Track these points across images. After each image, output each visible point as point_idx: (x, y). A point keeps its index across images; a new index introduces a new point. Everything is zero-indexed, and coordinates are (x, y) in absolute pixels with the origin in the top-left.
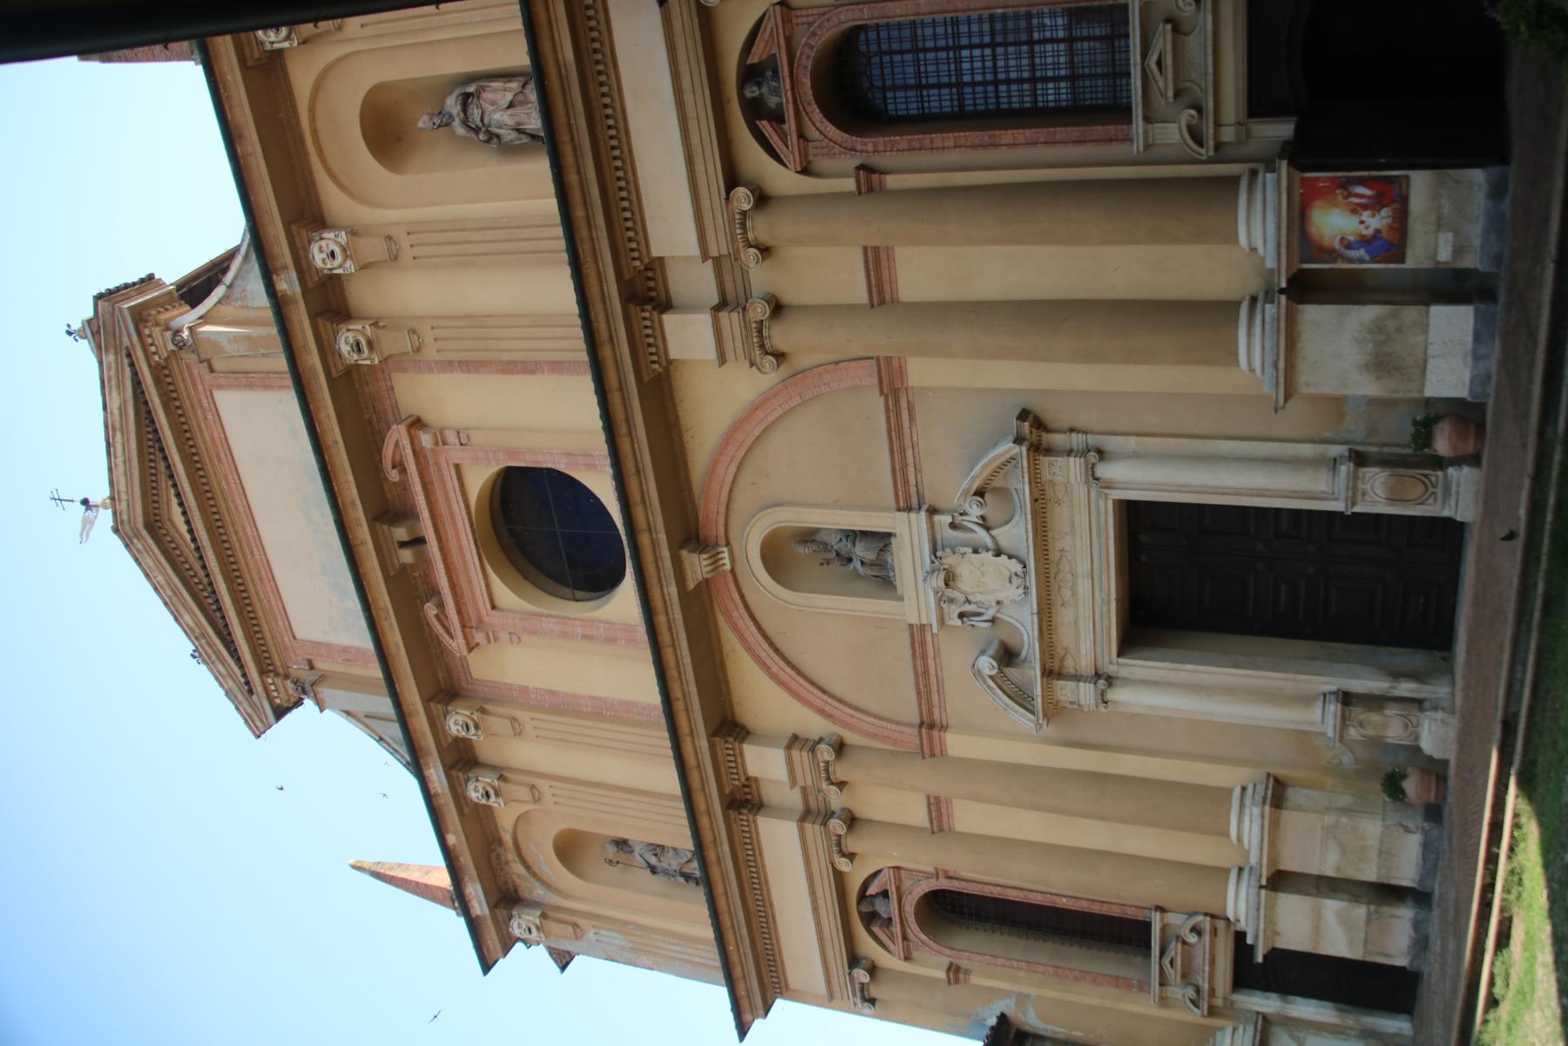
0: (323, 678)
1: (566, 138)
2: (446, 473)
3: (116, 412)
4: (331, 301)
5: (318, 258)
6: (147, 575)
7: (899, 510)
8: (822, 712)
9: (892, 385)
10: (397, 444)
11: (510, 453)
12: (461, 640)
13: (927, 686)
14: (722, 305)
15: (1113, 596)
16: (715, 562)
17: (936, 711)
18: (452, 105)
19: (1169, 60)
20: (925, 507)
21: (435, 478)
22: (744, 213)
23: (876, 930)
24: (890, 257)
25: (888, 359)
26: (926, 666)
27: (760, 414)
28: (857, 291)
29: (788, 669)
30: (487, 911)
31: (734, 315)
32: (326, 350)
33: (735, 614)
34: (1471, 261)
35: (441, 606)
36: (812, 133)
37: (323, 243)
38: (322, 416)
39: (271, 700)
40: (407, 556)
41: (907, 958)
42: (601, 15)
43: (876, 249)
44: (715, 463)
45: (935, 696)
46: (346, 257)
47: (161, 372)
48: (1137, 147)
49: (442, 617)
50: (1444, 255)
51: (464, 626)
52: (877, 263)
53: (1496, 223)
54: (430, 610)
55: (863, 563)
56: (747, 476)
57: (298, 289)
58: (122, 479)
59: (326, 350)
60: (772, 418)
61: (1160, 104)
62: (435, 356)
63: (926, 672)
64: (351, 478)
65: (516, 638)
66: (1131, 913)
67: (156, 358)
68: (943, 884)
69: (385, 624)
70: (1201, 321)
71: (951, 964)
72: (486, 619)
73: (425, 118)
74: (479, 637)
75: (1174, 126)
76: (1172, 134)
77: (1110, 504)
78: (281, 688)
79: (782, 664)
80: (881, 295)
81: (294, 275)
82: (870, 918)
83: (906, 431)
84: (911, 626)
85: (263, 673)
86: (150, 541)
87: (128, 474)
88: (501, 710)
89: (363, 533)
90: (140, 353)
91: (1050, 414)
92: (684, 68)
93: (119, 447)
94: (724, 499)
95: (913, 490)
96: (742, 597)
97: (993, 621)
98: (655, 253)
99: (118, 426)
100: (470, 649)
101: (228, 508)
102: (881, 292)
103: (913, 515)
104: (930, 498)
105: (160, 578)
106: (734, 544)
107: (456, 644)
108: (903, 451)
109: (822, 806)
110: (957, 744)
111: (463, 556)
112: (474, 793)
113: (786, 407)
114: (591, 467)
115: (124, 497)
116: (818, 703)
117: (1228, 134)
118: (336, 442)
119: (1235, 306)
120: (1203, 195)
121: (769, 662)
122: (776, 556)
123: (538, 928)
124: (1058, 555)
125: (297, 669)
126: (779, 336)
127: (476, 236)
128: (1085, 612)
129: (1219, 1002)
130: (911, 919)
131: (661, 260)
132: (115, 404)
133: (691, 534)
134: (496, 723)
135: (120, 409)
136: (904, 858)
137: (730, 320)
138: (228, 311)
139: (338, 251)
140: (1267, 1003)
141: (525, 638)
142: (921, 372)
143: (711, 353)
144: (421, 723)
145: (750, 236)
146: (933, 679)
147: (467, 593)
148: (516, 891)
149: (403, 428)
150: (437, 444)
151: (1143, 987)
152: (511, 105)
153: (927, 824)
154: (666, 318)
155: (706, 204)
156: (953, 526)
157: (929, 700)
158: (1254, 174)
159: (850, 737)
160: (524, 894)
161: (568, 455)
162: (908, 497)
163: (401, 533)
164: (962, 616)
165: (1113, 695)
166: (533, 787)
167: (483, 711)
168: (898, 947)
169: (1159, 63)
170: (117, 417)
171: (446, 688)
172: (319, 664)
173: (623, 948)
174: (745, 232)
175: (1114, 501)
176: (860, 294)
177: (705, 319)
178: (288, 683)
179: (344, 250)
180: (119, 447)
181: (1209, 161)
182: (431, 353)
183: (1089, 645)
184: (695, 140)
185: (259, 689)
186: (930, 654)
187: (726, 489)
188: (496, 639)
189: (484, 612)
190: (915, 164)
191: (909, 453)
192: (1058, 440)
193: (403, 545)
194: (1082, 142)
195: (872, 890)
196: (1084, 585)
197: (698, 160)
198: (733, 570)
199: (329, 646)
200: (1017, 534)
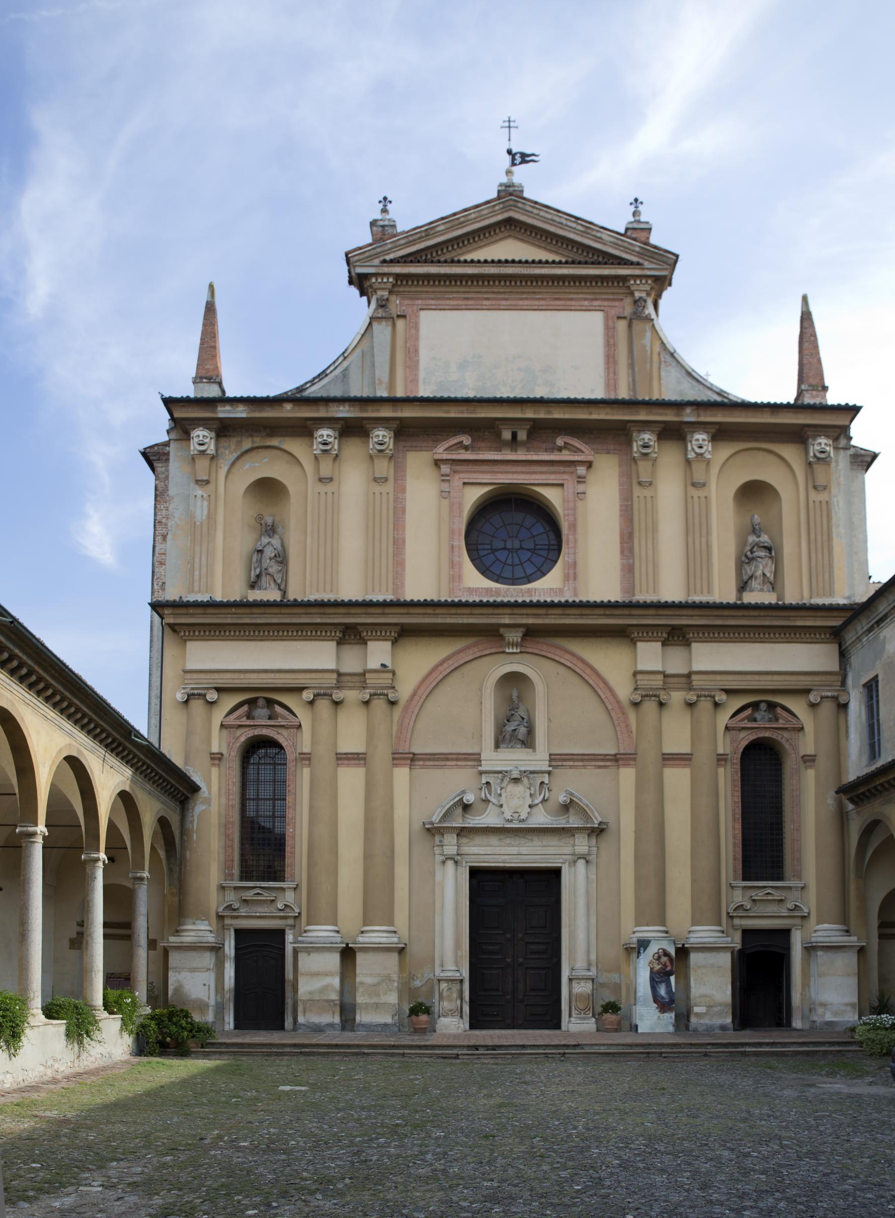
0: (394, 325)
1: (762, 614)
2: (558, 476)
3: (599, 235)
4: (674, 434)
5: (701, 437)
6: (477, 206)
7: (550, 755)
8: (414, 694)
9: (617, 760)
10: (583, 452)
11: (573, 527)
12: (445, 457)
13: (438, 760)
14: (666, 676)
15: (507, 865)
16: (514, 645)
17: (421, 763)
18: (765, 538)
20: (551, 769)
21: (555, 468)
22: (713, 697)
23: (245, 708)
25: (635, 759)
26: (452, 760)
27: (602, 685)
29: (441, 677)
30: (221, 415)
31: (661, 683)
32: (645, 425)
33: (476, 649)
35: (466, 448)
37: (706, 443)
38: (609, 410)
39: (376, 275)
40: (507, 435)
41: (222, 726)
42: (810, 640)
43: (690, 760)
44: (573, 655)
45: (431, 763)
46: (698, 454)
48: (734, 883)
49: (460, 446)
51: (454, 460)
54: (467, 440)
55: (515, 730)
56: (562, 670)
57: (686, 419)
58: (549, 216)
59: (645, 425)
60: (599, 691)
61: (753, 893)
62: (635, 495)
63: (447, 759)
64: (567, 416)
65: (444, 495)
66: (288, 869)
67: (632, 282)
68: (290, 755)
69: (464, 408)
70: (655, 908)
71: (222, 754)
72: (457, 476)
73: (759, 520)
74: (445, 469)
75: (740, 899)
76: (738, 897)
77: (560, 865)
78: (383, 286)
79: (445, 673)
80: (670, 759)
81: (692, 419)
82: (252, 702)
83: (593, 763)
84: (480, 754)
85: (397, 276)
86: (500, 218)
87: (552, 222)
88: (392, 471)
89: (530, 414)
92: (782, 678)
93: (574, 225)
94: (549, 655)
95: (560, 763)
96: (486, 655)
97: (486, 801)
98: (694, 645)
99: (589, 231)
100: (437, 463)
102: (668, 759)
103: (547, 763)
104: (557, 771)
105: (473, 216)
106: (520, 655)
107: (441, 451)
108: (582, 760)
109: (344, 684)
110: (402, 774)
111: (501, 473)
112: (325, 433)
113: (605, 700)
114: (566, 578)
115: (535, 211)
116: (420, 692)
118: (590, 414)
120: (708, 908)
121: (445, 665)
122: (514, 681)
123: (203, 452)
124: (530, 837)
125: (396, 304)
126: (650, 706)
127: (704, 540)
128: (497, 850)
129: (228, 921)
130: (257, 732)
131: (688, 645)
133: (531, 633)
134: (383, 467)
135: (600, 238)
136: (307, 732)
137: (658, 681)
139: (702, 451)
140: (230, 948)
141: (445, 503)
142: (627, 775)
143: (641, 667)
144: (386, 412)
145: (703, 698)
146: (443, 763)
147: (476, 468)
148: (225, 436)
149: (590, 458)
150: (579, 477)
151: (229, 876)
152: (764, 575)
153: (339, 751)
154: (660, 644)
155: (718, 677)
156: (542, 783)
157: (429, 760)
158: (723, 932)
159: (397, 712)
160: (223, 440)
161: (575, 563)
162: (555, 760)
163: (522, 436)
164: (488, 783)
165: (450, 863)
166: (331, 479)
167: (391, 458)
168: (231, 720)
169: (768, 893)
170: (594, 233)
171: (405, 432)
172: (400, 323)
173: (191, 516)
174: (705, 696)
175: (561, 868)
176: (667, 749)
177: (660, 669)
178: (386, 293)
179: (701, 454)
180: (574, 225)
181: (728, 913)
182: (637, 491)
183: (477, 852)
184: (749, 677)
186: (459, 763)
187: (557, 658)
188: (443, 480)
189: (463, 475)
191: (581, 763)
193: (514, 435)
195: (278, 709)
196: (514, 850)
197: (740, 677)
198: (504, 652)
199: (417, 338)
200: (541, 818)
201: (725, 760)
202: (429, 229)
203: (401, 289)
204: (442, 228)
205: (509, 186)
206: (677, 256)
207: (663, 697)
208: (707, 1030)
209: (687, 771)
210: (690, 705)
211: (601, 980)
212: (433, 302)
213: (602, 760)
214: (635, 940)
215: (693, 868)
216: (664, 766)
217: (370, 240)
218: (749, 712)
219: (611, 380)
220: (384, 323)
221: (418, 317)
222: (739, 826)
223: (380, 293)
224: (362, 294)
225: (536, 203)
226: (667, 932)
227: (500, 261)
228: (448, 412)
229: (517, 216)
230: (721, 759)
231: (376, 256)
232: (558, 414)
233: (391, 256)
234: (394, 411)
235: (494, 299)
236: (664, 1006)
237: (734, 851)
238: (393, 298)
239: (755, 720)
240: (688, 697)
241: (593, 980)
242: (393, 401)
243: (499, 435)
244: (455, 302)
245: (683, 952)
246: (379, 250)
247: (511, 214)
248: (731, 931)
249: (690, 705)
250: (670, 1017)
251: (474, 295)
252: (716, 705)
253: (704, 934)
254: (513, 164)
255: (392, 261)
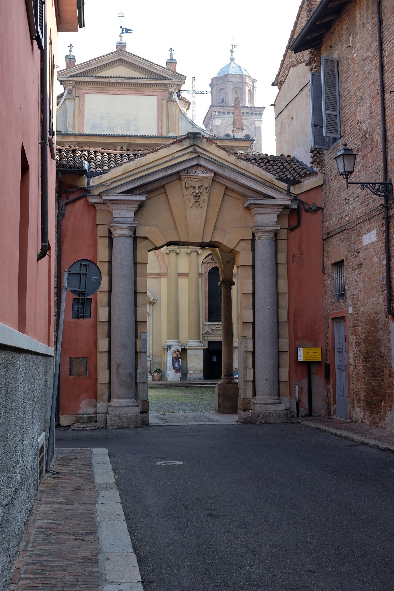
6: (108, 55)
19: (219, 329)
22: (197, 251)
24: (186, 278)
25: (167, 275)
28: (180, 271)
34: (188, 376)
36: (209, 265)
47: (165, 85)
48: (205, 323)
50: (190, 372)
52: (186, 275)
53: (195, 379)
61: (213, 327)
64: (142, 142)
76: (207, 329)
78: (70, 85)
80: (180, 275)
86: (117, 58)
89: (128, 141)
90: (170, 82)
91: (155, 305)
93: (146, 63)
101: (126, 88)
115: (131, 57)
117: (206, 338)
119: (178, 338)
125: (75, 92)
132: (158, 68)
138: (178, 112)
142: (164, 281)
172: (77, 99)
180: (146, 63)
185: (71, 79)
190: (203, 284)
192: (151, 306)
193: (122, 148)
194: (205, 313)
201: (202, 275)
202: (88, 63)
203: (77, 86)
204: (94, 62)
205: (121, 44)
206: (186, 77)
207: (178, 252)
208: (194, 380)
209: (187, 279)
210: (189, 254)
211: (154, 361)
212: (90, 91)
213: (155, 275)
214: (166, 345)
215: (189, 317)
216: (178, 277)
217: (65, 68)
218: (211, 256)
219: (160, 126)
220: (71, 100)
221: (84, 97)
222: (207, 301)
223: (69, 87)
224: (61, 84)
225: (131, 54)
226: (179, 342)
227: (116, 77)
228: (96, 140)
229: (123, 58)
230: (200, 275)
231: (68, 73)
232: (138, 141)
233: (74, 73)
234: (75, 139)
235: (114, 90)
236: (177, 370)
237: (205, 311)
238: (74, 89)
239: (214, 260)
240: (187, 251)
241: (151, 361)
242: (75, 135)
243: (116, 147)
244: (99, 91)
245: (184, 350)
246: (69, 71)
247: (121, 56)
248: (204, 342)
249: (189, 254)
250: (179, 375)
251: (106, 89)
252: (198, 254)
253: (193, 343)
254: (122, 33)
255: (74, 76)
